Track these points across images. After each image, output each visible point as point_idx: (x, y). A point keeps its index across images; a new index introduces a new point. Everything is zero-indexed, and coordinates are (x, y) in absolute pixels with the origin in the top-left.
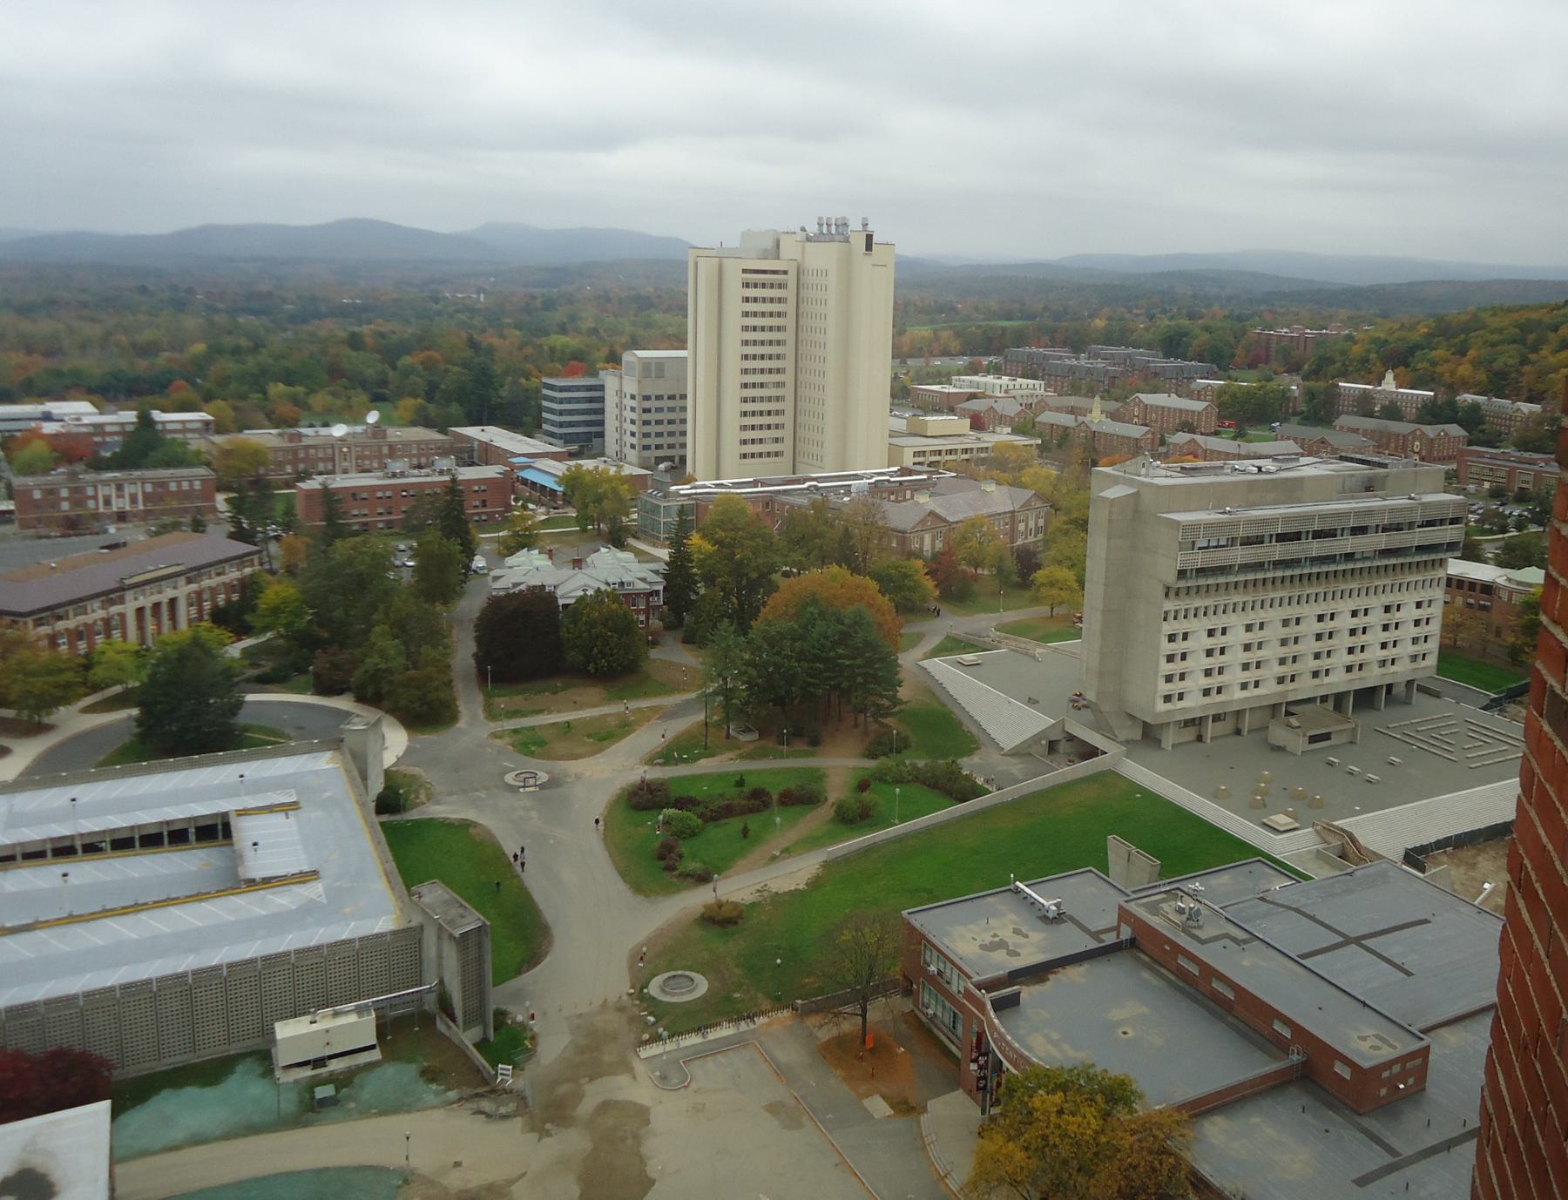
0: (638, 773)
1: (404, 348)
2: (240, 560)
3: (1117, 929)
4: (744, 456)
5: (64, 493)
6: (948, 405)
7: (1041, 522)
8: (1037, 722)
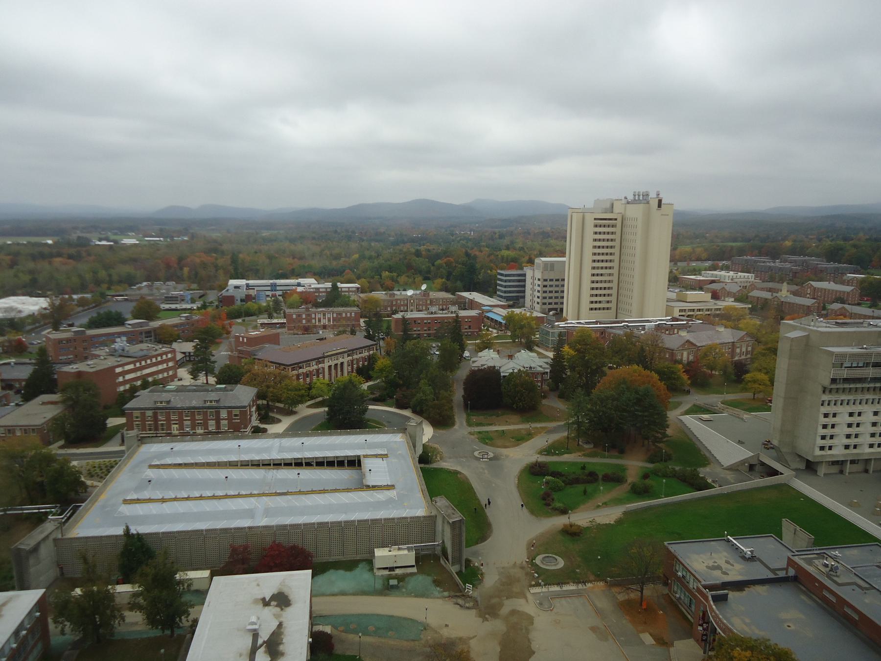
0: (535, 458)
1: (438, 256)
2: (368, 348)
3: (786, 569)
4: (591, 309)
5: (304, 316)
6: (699, 286)
7: (750, 349)
8: (744, 454)
